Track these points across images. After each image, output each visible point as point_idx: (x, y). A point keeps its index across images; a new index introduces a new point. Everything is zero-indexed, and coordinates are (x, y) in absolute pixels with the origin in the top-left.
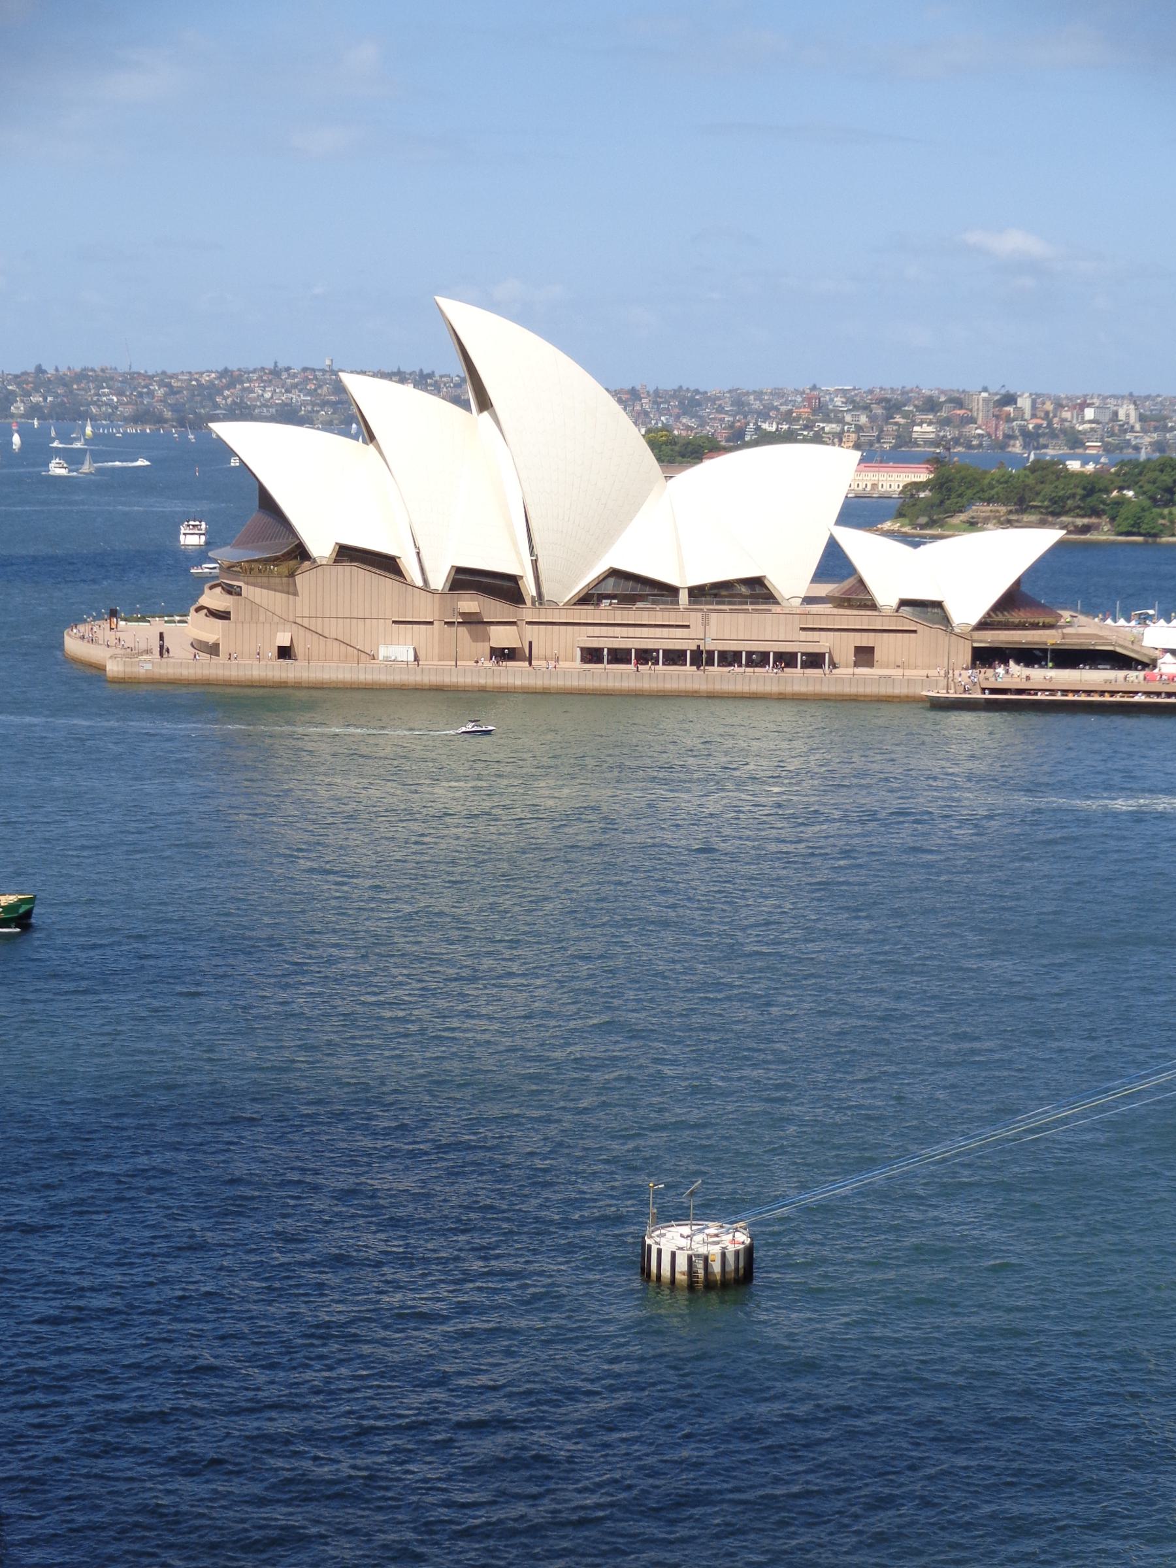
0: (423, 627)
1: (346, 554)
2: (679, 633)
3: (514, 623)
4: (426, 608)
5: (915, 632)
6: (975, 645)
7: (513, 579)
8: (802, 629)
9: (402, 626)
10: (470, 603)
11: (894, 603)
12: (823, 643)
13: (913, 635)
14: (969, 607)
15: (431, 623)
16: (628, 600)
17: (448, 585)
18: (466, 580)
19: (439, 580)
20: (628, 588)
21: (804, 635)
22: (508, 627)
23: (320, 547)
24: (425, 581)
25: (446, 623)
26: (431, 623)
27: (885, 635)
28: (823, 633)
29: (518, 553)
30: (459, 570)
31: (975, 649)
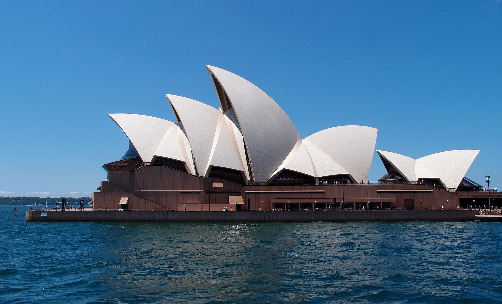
0: (195, 195)
1: (158, 160)
2: (320, 196)
9: (185, 195)
11: (416, 180)
12: (391, 199)
13: (431, 194)
14: (452, 182)
16: (292, 183)
17: (209, 176)
18: (216, 172)
19: (204, 173)
21: (379, 196)
23: (147, 159)
24: (197, 173)
29: (241, 161)
31: (461, 200)
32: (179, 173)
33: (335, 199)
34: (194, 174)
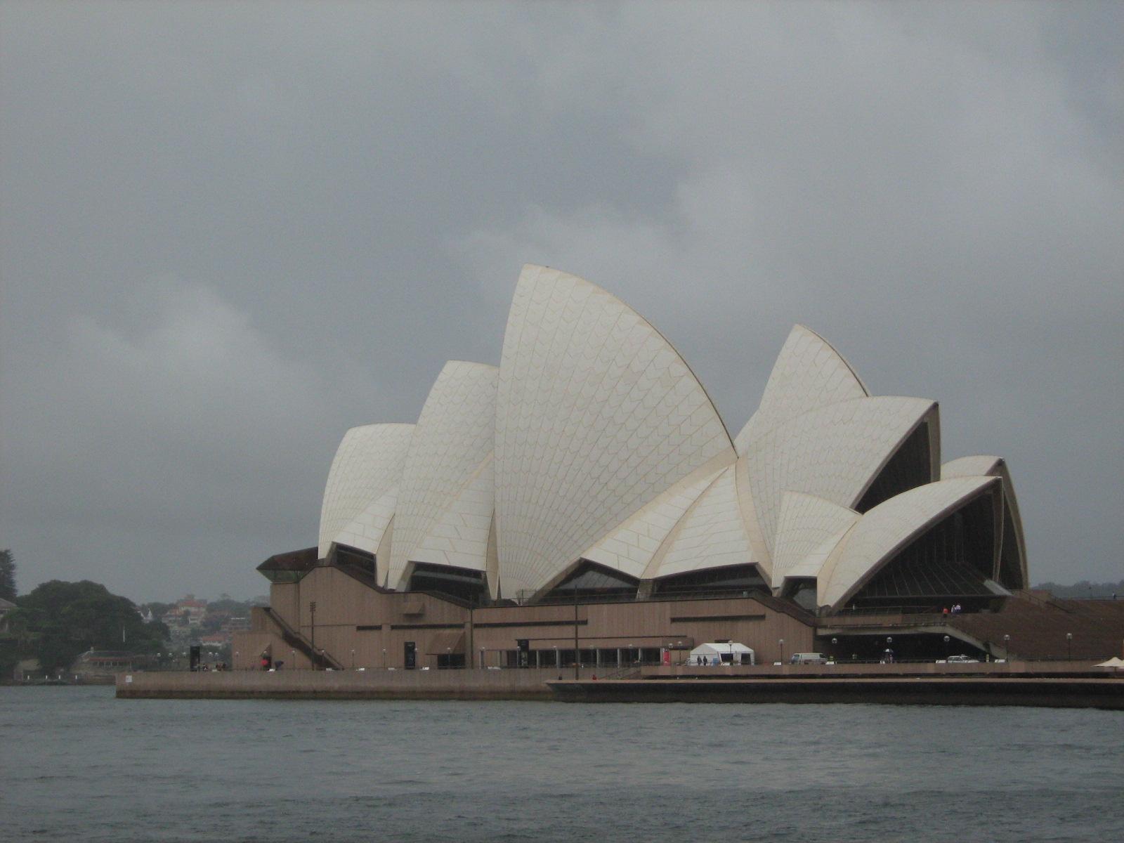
3: (461, 626)
4: (375, 610)
5: (762, 617)
6: (821, 632)
7: (476, 574)
8: (674, 620)
10: (414, 603)
13: (762, 623)
15: (379, 628)
20: (612, 583)
21: (674, 625)
22: (455, 631)
25: (393, 628)
26: (379, 628)
27: (740, 624)
28: (690, 624)
30: (420, 566)
32: (354, 584)
33: (524, 644)
34: (380, 582)
